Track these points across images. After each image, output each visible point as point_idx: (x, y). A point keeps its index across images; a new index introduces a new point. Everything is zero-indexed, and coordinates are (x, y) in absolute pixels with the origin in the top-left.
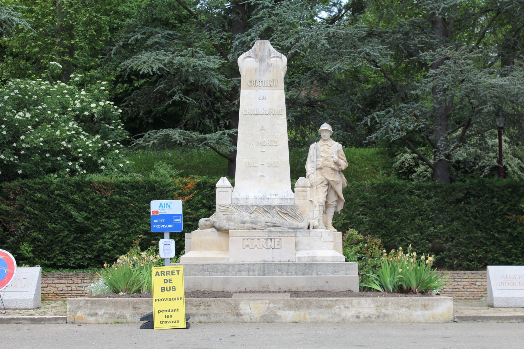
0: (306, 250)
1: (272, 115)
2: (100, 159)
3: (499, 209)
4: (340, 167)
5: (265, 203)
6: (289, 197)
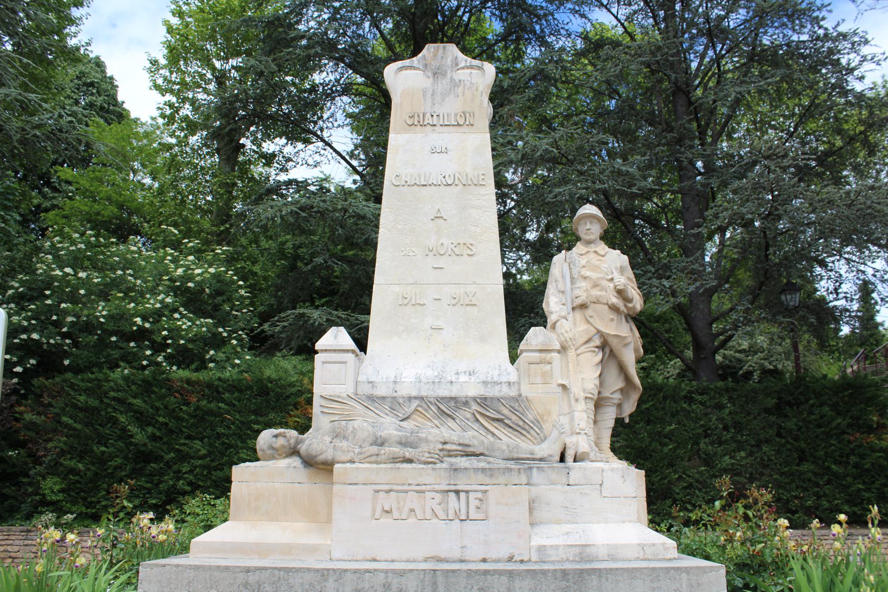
0: (558, 522)
1: (461, 186)
2: (208, 352)
3: (834, 424)
4: (630, 305)
5: (444, 392)
6: (504, 379)
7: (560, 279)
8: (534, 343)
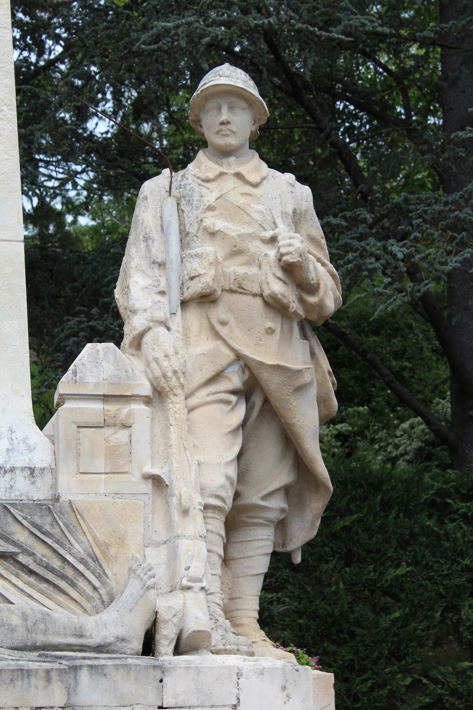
4: (312, 300)
7: (155, 235)
8: (91, 378)
